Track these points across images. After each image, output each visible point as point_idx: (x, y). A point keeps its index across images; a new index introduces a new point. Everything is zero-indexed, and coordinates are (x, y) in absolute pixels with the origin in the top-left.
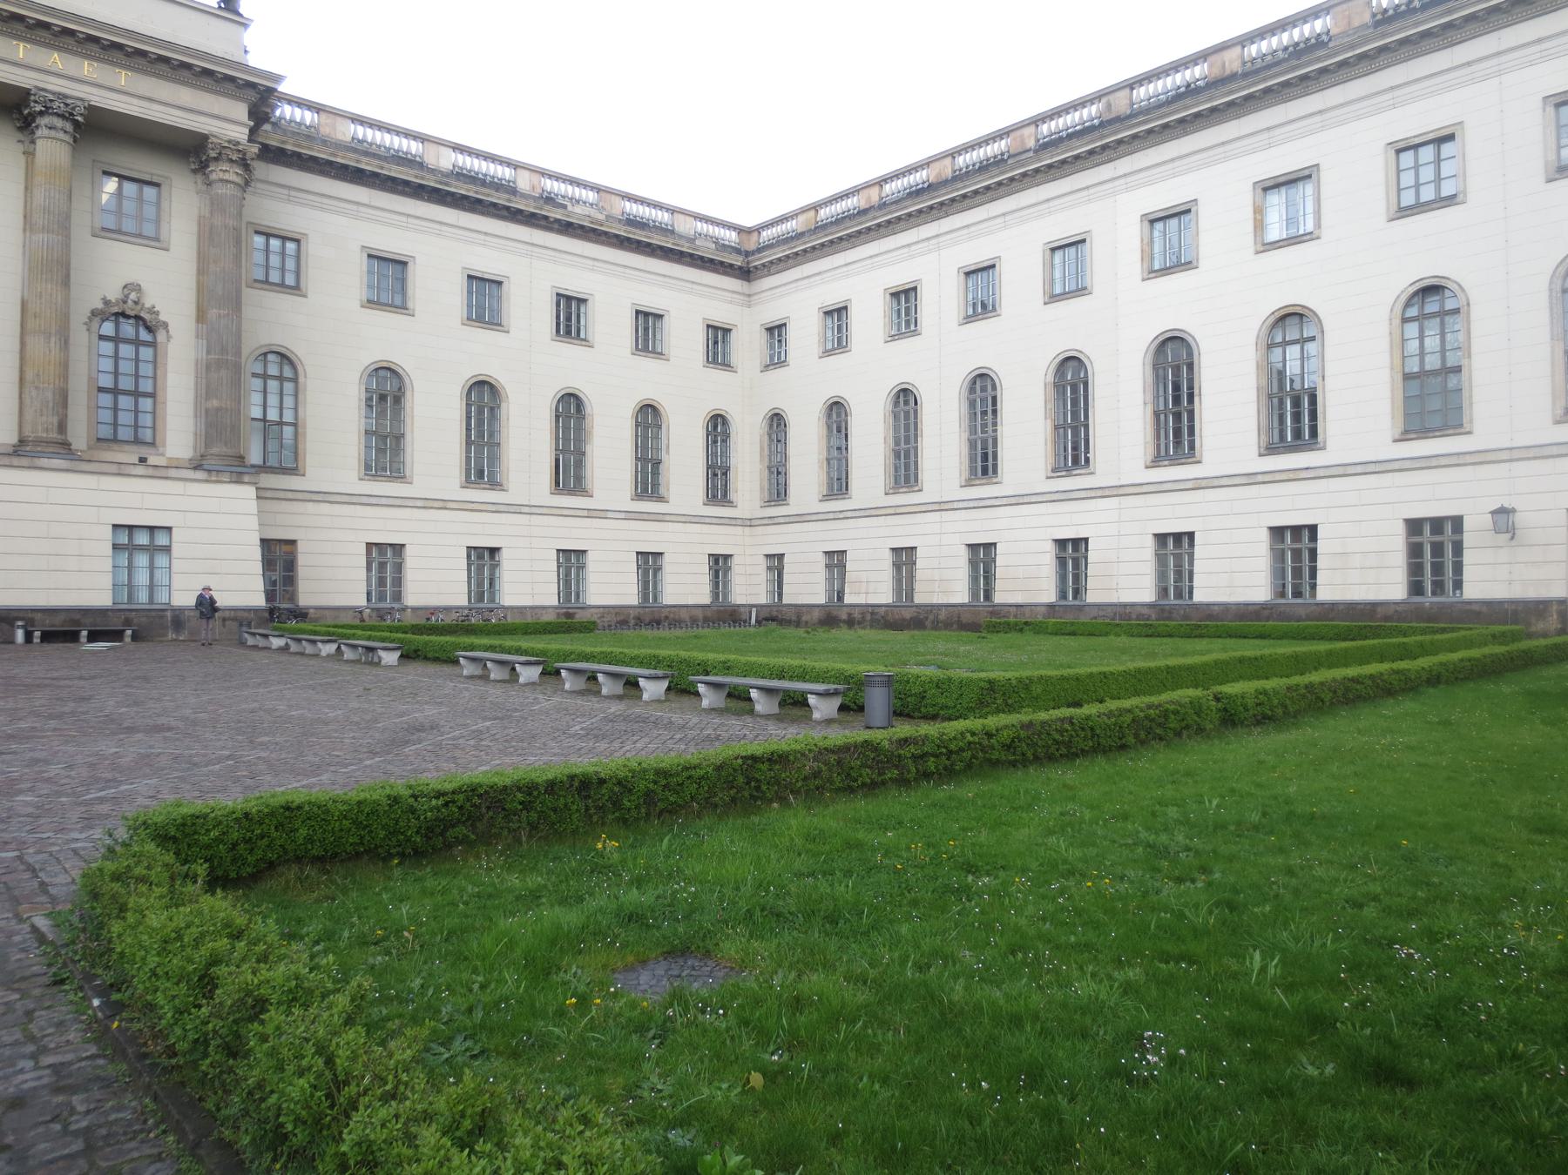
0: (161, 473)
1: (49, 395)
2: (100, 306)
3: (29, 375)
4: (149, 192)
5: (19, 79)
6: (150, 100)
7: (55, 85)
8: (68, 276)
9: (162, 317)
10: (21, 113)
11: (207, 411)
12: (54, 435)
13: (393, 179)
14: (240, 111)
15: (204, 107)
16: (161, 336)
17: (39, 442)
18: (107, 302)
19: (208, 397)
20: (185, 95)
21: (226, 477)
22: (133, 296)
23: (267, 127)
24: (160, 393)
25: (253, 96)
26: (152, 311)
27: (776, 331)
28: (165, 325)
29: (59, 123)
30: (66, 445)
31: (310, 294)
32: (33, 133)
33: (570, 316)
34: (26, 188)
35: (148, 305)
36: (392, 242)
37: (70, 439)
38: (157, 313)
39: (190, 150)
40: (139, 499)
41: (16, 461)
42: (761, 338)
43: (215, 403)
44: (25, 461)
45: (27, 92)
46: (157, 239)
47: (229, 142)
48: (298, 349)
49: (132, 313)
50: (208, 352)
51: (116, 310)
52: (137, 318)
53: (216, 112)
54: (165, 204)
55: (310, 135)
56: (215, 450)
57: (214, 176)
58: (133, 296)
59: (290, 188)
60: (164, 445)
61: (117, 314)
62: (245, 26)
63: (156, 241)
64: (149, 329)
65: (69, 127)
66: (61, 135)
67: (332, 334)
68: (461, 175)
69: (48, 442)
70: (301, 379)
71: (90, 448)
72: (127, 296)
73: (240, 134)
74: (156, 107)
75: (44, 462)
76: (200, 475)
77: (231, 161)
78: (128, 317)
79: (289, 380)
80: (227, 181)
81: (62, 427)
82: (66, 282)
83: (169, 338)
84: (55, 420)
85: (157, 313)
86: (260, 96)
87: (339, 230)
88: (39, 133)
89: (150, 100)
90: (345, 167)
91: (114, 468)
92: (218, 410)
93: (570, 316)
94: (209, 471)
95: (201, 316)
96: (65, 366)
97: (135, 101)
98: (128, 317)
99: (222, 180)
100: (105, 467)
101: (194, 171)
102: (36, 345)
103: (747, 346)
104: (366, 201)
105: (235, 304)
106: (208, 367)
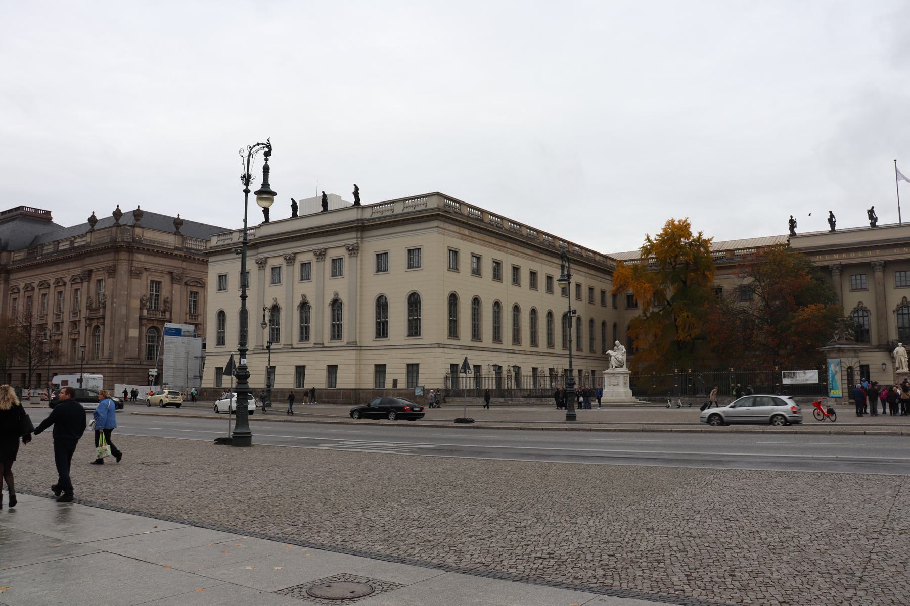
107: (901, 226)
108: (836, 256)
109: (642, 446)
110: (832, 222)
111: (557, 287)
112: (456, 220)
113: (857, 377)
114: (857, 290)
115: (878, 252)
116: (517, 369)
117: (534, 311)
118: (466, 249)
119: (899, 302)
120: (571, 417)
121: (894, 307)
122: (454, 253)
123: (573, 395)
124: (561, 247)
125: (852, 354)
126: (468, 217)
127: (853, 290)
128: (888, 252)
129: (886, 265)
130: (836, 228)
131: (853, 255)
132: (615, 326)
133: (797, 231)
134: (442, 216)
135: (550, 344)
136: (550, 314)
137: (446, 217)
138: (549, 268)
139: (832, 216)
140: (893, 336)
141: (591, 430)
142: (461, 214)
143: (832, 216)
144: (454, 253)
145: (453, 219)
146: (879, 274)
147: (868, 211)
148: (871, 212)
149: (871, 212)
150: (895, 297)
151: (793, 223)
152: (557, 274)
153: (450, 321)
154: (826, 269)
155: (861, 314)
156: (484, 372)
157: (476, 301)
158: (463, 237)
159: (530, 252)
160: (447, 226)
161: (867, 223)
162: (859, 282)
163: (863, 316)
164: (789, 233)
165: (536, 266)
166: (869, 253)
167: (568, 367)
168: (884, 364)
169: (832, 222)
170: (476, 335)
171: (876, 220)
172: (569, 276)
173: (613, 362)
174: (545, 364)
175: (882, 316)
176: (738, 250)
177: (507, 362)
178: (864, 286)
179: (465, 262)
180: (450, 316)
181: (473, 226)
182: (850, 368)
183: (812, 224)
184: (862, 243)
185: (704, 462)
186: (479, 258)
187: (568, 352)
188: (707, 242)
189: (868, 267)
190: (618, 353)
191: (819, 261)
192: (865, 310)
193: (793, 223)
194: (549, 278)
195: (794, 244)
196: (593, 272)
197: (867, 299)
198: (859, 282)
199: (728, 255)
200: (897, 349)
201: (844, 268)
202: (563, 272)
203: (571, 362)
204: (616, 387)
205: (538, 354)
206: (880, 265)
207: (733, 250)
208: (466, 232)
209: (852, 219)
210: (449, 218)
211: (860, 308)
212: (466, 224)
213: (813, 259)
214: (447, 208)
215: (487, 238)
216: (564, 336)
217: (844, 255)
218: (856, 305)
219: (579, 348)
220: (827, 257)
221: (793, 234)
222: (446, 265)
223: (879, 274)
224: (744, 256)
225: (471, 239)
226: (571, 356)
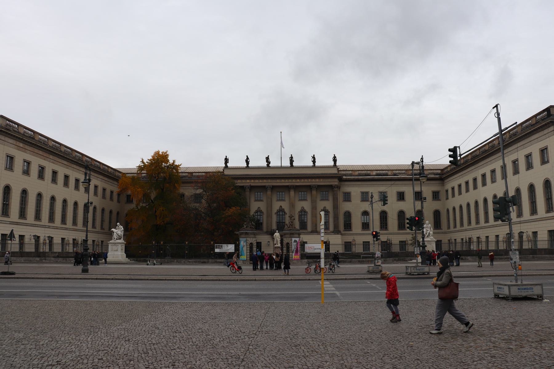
7: (314, 184)
14: (337, 180)
20: (329, 180)
27: (447, 191)
33: (401, 196)
36: (365, 189)
39: (331, 187)
42: (445, 192)
48: (351, 211)
67: (356, 207)
68: (377, 175)
81: (316, 229)
87: (355, 190)
93: (401, 196)
96: (316, 221)
103: (442, 195)
107: (281, 167)
108: (248, 181)
109: (128, 289)
110: (247, 162)
111: (82, 188)
112: (14, 136)
113: (255, 249)
115: (269, 181)
116: (51, 239)
117: (65, 201)
118: (20, 156)
119: (278, 208)
120: (85, 271)
121: (276, 211)
122: (11, 159)
123: (87, 257)
124: (86, 161)
125: (253, 236)
126: (24, 135)
127: (256, 200)
128: (274, 181)
129: (273, 188)
132: (118, 213)
133: (229, 165)
134: (4, 132)
135: (75, 223)
136: (76, 204)
137: (6, 133)
138: (76, 174)
139: (248, 158)
140: (274, 227)
141: (97, 279)
142: (19, 132)
143: (248, 158)
144: (11, 159)
145: (12, 135)
146: (269, 193)
147: (266, 158)
148: (267, 158)
149: (267, 158)
150: (276, 206)
151: (226, 160)
152: (82, 178)
153: (4, 204)
154: (242, 187)
155: (259, 214)
156: (26, 240)
157: (24, 192)
158: (19, 148)
159: (65, 163)
160: (7, 139)
161: (265, 164)
162: (259, 196)
163: (260, 215)
164: (224, 165)
165: (68, 172)
166: (265, 181)
167: (85, 238)
169: (247, 162)
170: (23, 214)
171: (269, 163)
172: (90, 180)
173: (115, 236)
174: (70, 236)
175: (269, 216)
176: (195, 173)
177: (43, 234)
179: (19, 165)
180: (4, 201)
181: (26, 141)
182: (251, 244)
183: (237, 162)
184: (262, 175)
185: (165, 298)
186: (29, 163)
187: (85, 229)
188: (178, 166)
189: (264, 188)
190: (119, 231)
191: (239, 183)
192: (261, 212)
193: (226, 160)
194: (77, 181)
195: (227, 172)
196: (106, 179)
197: (262, 206)
198: (259, 196)
199: (189, 175)
201: (252, 188)
202: (85, 177)
203: (87, 235)
204: (116, 252)
205: (66, 229)
207: (192, 173)
208: (21, 145)
209: (258, 162)
210: (9, 134)
211: (259, 211)
212: (22, 139)
213: (236, 181)
214: (8, 127)
215: (36, 151)
216: (84, 218)
217: (252, 181)
218: (256, 209)
219: (94, 226)
220: (243, 181)
221: (226, 166)
222: (4, 166)
223: (269, 193)
224: (198, 176)
225: (25, 150)
226: (87, 231)
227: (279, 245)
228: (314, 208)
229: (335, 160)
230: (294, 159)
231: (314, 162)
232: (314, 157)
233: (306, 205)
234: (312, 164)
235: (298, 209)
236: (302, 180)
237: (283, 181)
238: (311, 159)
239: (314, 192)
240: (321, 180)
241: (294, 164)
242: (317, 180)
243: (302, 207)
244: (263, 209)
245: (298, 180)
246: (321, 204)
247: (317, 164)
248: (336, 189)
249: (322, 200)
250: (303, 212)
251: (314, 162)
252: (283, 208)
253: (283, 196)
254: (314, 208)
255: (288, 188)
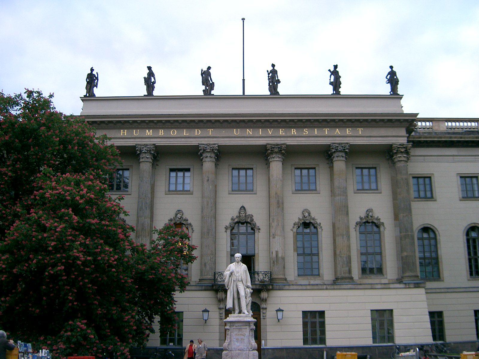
0: (386, 287)
1: (345, 259)
2: (359, 220)
3: (338, 252)
4: (372, 171)
5: (327, 141)
6: (370, 137)
7: (338, 140)
8: (348, 211)
9: (381, 221)
10: (327, 153)
11: (402, 257)
12: (347, 275)
13: (467, 142)
14: (403, 132)
15: (390, 134)
16: (382, 229)
17: (343, 278)
18: (361, 218)
19: (402, 251)
20: (383, 132)
21: (412, 286)
22: (370, 214)
23: (413, 134)
24: (383, 252)
25: (407, 124)
26: (378, 219)
28: (383, 224)
29: (340, 154)
30: (352, 278)
31: (438, 199)
32: (332, 160)
34: (331, 180)
35: (376, 217)
37: (353, 276)
38: (379, 219)
40: (381, 299)
41: (335, 287)
43: (405, 254)
44: (338, 287)
45: (329, 146)
46: (377, 189)
47: (400, 145)
49: (371, 221)
50: (400, 232)
51: (364, 221)
52: (373, 222)
53: (394, 135)
54: (378, 176)
55: (429, 132)
56: (407, 274)
57: (396, 160)
58: (370, 214)
59: (424, 156)
60: (386, 275)
61: (365, 223)
62: (401, 98)
63: (377, 190)
64: (378, 226)
65: (344, 155)
66: (342, 158)
69: (345, 278)
70: (438, 238)
71: (359, 278)
72: (368, 215)
73: (404, 141)
74: (372, 139)
75: (344, 287)
76: (402, 286)
77: (402, 152)
78: (369, 223)
79: (432, 239)
80: (401, 161)
81: (350, 272)
82: (347, 214)
83: (385, 228)
84: (347, 269)
85: (379, 219)
86: (409, 122)
88: (334, 159)
89: (370, 137)
90: (446, 141)
91: (369, 286)
92: (407, 256)
94: (405, 284)
95: (396, 217)
96: (349, 247)
97: (365, 139)
98: (369, 223)
99: (399, 161)
100: (367, 286)
101: (388, 160)
102: (339, 240)
104: (456, 154)
105: (409, 210)
106: (401, 239)
107: (244, 97)
108: (149, 133)
114: (176, 192)
115: (210, 132)
119: (235, 214)
127: (169, 192)
128: (224, 132)
129: (222, 154)
130: (156, 93)
131: (174, 133)
143: (151, 74)
148: (206, 76)
149: (206, 76)
161: (199, 90)
162: (180, 180)
166: (197, 132)
168: (206, 311)
178: (187, 188)
189: (194, 153)
191: (122, 138)
193: (92, 80)
197: (189, 207)
198: (180, 180)
200: (232, 266)
206: (212, 151)
218: (172, 216)
227: (247, 316)
228: (341, 209)
229: (393, 79)
230: (280, 76)
231: (336, 84)
232: (335, 73)
233: (316, 204)
234: (329, 90)
235: (294, 216)
236: (306, 132)
237: (249, 132)
238: (327, 78)
239: (339, 164)
240: (360, 131)
241: (282, 90)
242: (348, 131)
243: (306, 210)
244: (192, 215)
245: (294, 132)
246: (361, 204)
247: (343, 91)
248: (402, 157)
249: (362, 190)
250: (307, 224)
251: (336, 84)
252: (249, 212)
253: (249, 180)
254: (341, 209)
255: (263, 154)
